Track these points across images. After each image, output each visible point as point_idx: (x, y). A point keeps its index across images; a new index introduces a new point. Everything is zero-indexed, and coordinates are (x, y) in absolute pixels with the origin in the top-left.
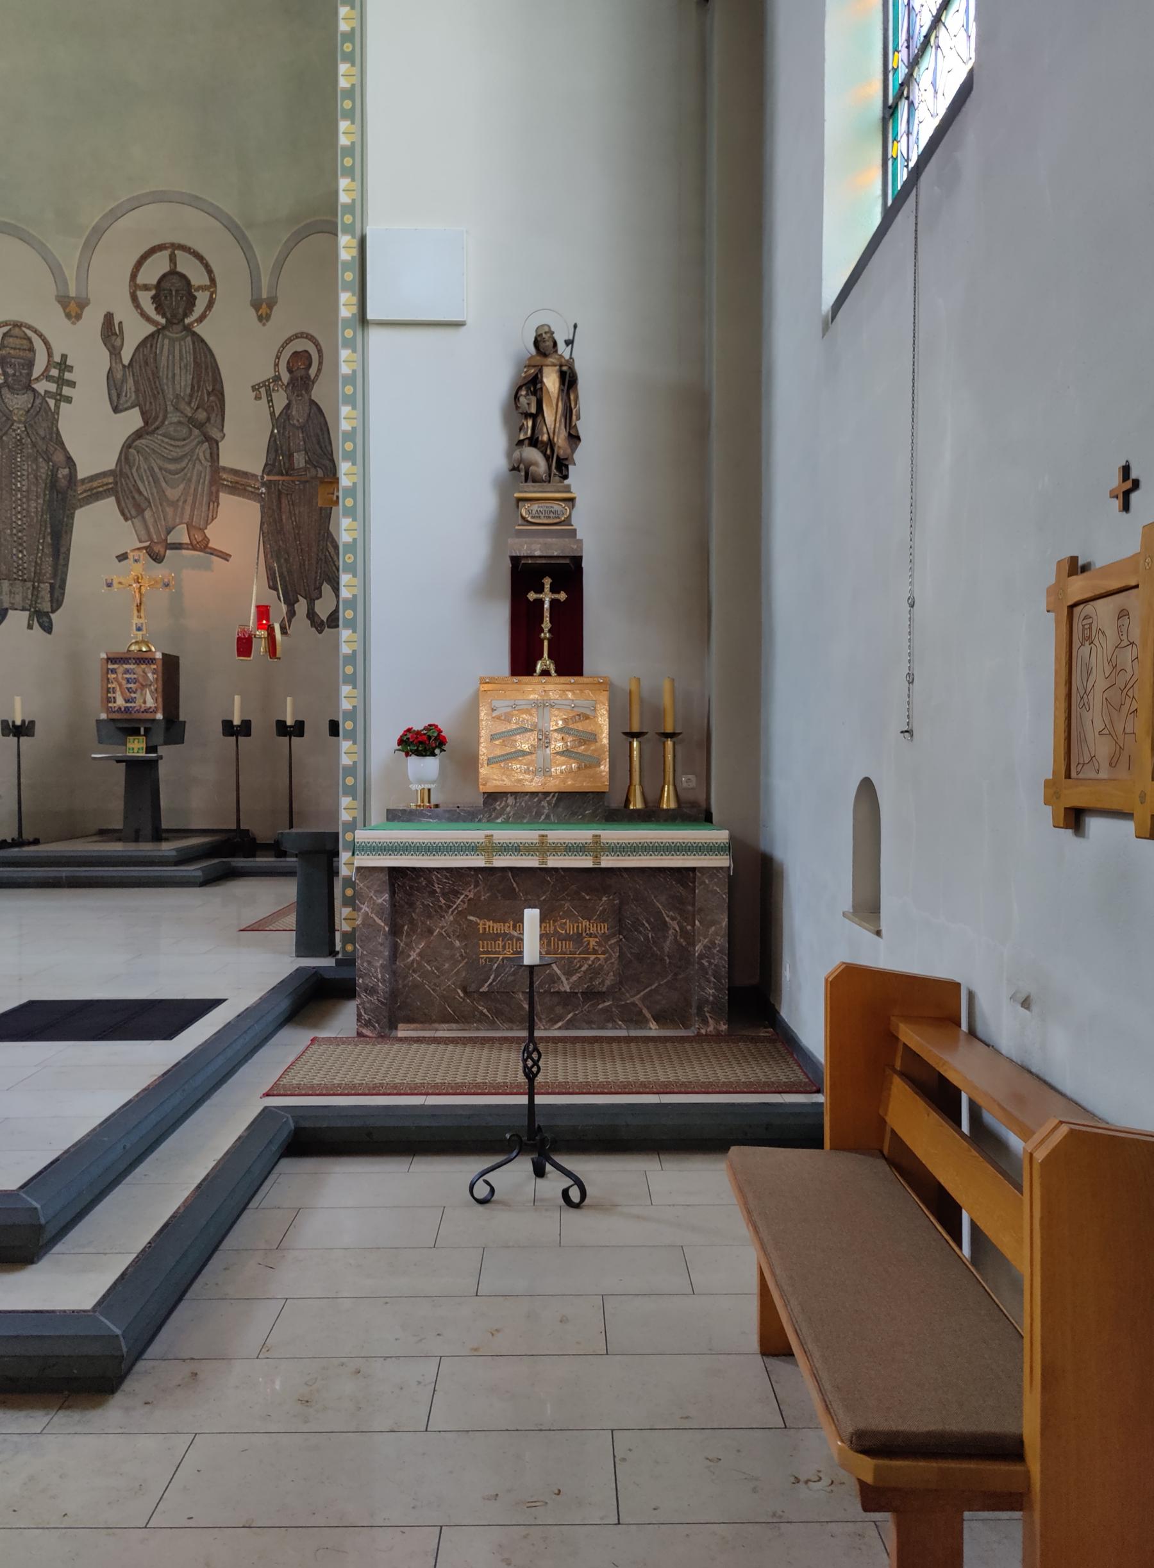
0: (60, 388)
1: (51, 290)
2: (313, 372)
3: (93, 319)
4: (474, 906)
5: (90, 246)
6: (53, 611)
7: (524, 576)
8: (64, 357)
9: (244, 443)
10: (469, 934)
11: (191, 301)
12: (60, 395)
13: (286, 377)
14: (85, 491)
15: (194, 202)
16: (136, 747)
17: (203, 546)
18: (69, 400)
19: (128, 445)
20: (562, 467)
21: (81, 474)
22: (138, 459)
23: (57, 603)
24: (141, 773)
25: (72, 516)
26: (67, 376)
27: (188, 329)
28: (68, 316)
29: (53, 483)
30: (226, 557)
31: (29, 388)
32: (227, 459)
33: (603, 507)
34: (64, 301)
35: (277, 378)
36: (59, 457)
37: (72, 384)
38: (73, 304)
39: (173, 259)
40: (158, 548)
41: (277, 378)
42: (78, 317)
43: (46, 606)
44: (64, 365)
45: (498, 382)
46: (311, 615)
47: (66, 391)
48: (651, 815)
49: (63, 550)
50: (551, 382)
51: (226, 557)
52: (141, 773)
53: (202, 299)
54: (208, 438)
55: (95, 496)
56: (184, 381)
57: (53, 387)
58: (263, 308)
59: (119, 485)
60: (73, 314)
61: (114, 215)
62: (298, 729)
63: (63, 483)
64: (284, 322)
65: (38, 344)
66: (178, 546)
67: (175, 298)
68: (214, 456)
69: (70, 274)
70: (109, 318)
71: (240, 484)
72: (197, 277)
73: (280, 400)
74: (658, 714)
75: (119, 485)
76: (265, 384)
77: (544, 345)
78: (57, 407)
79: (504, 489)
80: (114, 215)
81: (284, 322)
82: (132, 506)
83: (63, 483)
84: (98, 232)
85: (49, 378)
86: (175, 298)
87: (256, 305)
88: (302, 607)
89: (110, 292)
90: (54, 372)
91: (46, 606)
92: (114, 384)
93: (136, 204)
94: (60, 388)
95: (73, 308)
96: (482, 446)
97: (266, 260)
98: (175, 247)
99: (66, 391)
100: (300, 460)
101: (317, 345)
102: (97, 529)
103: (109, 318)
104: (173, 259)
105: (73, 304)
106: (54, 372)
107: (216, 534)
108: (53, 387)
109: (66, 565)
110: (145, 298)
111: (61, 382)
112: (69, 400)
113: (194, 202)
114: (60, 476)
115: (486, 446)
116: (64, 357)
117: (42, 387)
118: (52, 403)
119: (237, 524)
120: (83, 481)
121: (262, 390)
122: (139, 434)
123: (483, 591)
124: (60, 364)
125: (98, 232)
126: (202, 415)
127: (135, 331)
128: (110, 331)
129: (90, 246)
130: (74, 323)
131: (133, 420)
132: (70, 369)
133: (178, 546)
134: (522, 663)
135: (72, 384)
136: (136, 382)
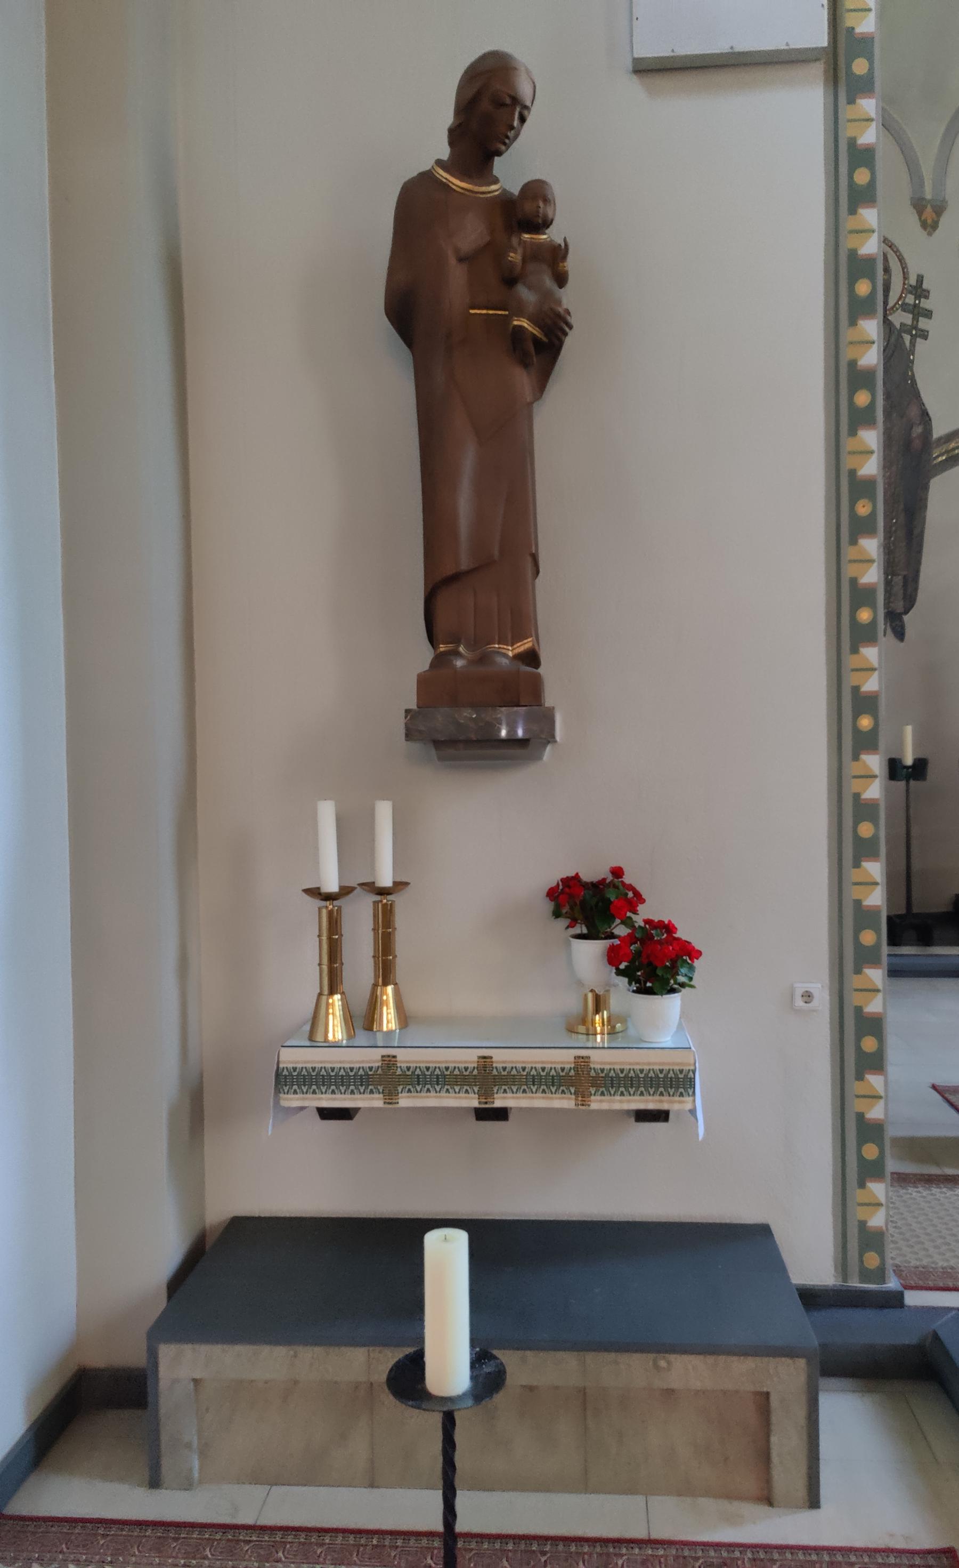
0: (915, 319)
6: (906, 612)
8: (920, 279)
12: (916, 328)
14: (942, 455)
18: (924, 335)
21: (939, 431)
23: (910, 601)
25: (926, 488)
26: (925, 304)
28: (924, 225)
34: (919, 205)
36: (914, 412)
37: (928, 314)
38: (929, 209)
42: (935, 226)
43: (899, 606)
44: (919, 290)
47: (923, 323)
49: (916, 532)
57: (907, 319)
60: (929, 221)
63: (917, 444)
69: (927, 170)
78: (913, 344)
83: (917, 444)
85: (905, 308)
90: (910, 299)
91: (899, 606)
94: (915, 319)
99: (923, 323)
105: (929, 209)
106: (910, 299)
108: (907, 319)
109: (920, 552)
111: (918, 312)
112: (924, 335)
114: (914, 435)
116: (920, 279)
118: (907, 338)
120: (939, 439)
124: (915, 288)
130: (930, 234)
132: (925, 294)
135: (928, 314)
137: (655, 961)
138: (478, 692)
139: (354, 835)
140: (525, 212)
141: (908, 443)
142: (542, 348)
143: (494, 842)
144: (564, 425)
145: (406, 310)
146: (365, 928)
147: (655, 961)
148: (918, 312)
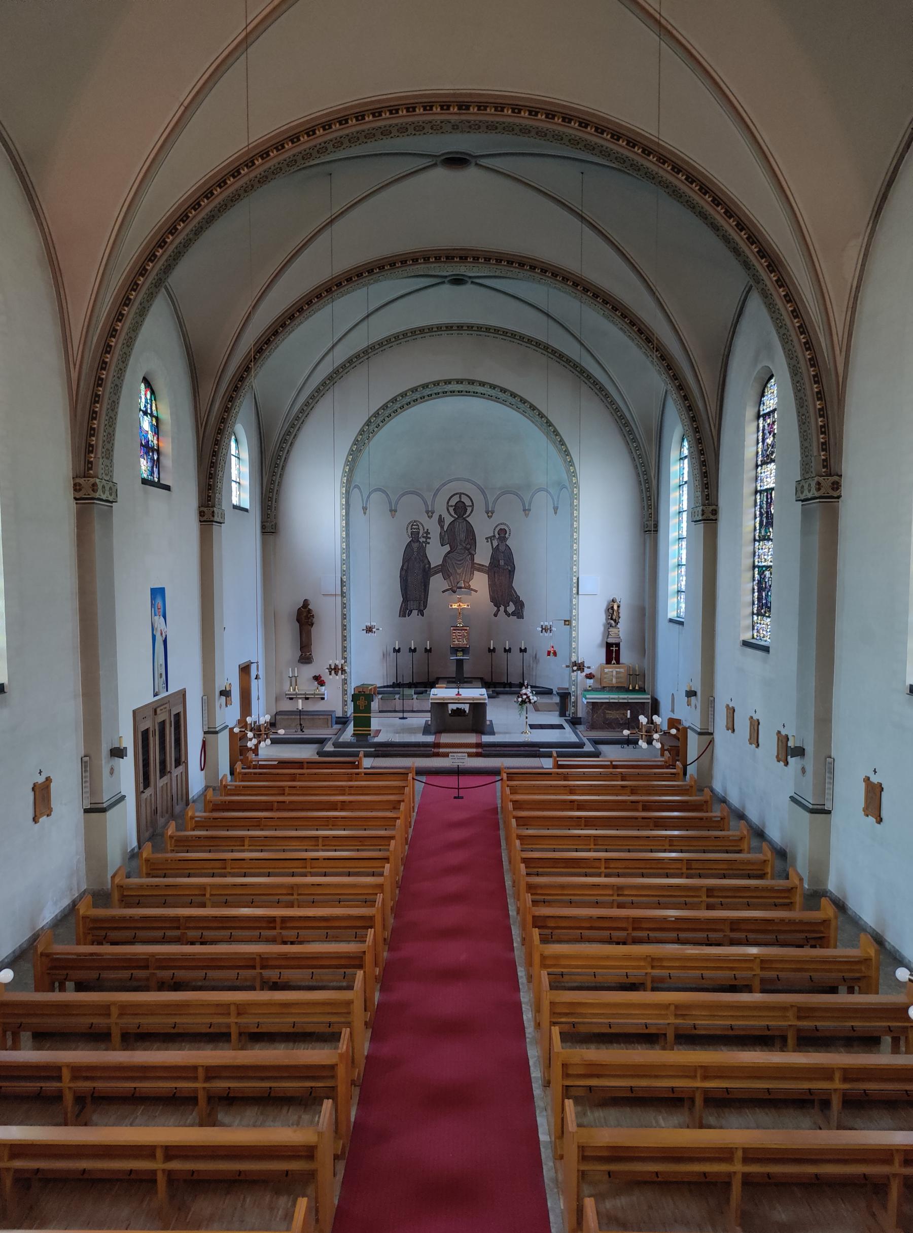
1: (424, 510)
2: (507, 536)
3: (436, 517)
4: (606, 708)
5: (435, 495)
7: (609, 646)
9: (483, 555)
10: (604, 713)
11: (466, 510)
13: (497, 536)
15: (468, 481)
16: (460, 656)
17: (469, 588)
19: (446, 556)
20: (617, 623)
22: (449, 561)
23: (425, 607)
24: (460, 663)
27: (464, 519)
29: (424, 570)
30: (476, 591)
31: (418, 541)
32: (477, 560)
33: (624, 631)
34: (427, 512)
35: (494, 536)
36: (426, 561)
39: (460, 497)
40: (455, 589)
41: (494, 536)
43: (422, 608)
44: (427, 533)
45: (604, 606)
46: (506, 611)
48: (634, 691)
50: (615, 608)
51: (476, 591)
52: (460, 663)
53: (469, 510)
54: (470, 554)
55: (436, 573)
56: (463, 536)
58: (490, 513)
59: (444, 569)
61: (444, 485)
62: (509, 650)
64: (497, 519)
65: (421, 527)
66: (461, 588)
67: (461, 509)
68: (473, 560)
69: (429, 503)
70: (440, 516)
71: (481, 568)
72: (468, 503)
73: (495, 543)
74: (634, 670)
75: (444, 569)
76: (490, 538)
77: (613, 601)
79: (604, 626)
80: (444, 485)
81: (497, 519)
82: (447, 576)
84: (438, 490)
86: (461, 509)
87: (487, 512)
88: (502, 608)
89: (441, 508)
91: (422, 608)
92: (442, 537)
93: (450, 481)
95: (430, 513)
96: (601, 618)
97: (491, 500)
98: (460, 494)
100: (502, 563)
101: (508, 526)
102: (437, 583)
103: (440, 516)
104: (460, 497)
107: (473, 584)
110: (451, 510)
111: (427, 538)
113: (468, 481)
115: (602, 618)
117: (421, 540)
119: (480, 582)
121: (490, 539)
122: (449, 553)
123: (601, 646)
125: (438, 490)
126: (468, 546)
127: (448, 520)
128: (441, 521)
129: (435, 495)
131: (447, 548)
133: (461, 588)
134: (608, 661)
136: (448, 536)
137: (322, 683)
138: (305, 657)
139: (293, 671)
140: (309, 611)
141: (424, 570)
142: (312, 624)
143: (308, 671)
144: (314, 630)
145: (298, 620)
146: (294, 680)
147: (322, 683)
148: (427, 538)
